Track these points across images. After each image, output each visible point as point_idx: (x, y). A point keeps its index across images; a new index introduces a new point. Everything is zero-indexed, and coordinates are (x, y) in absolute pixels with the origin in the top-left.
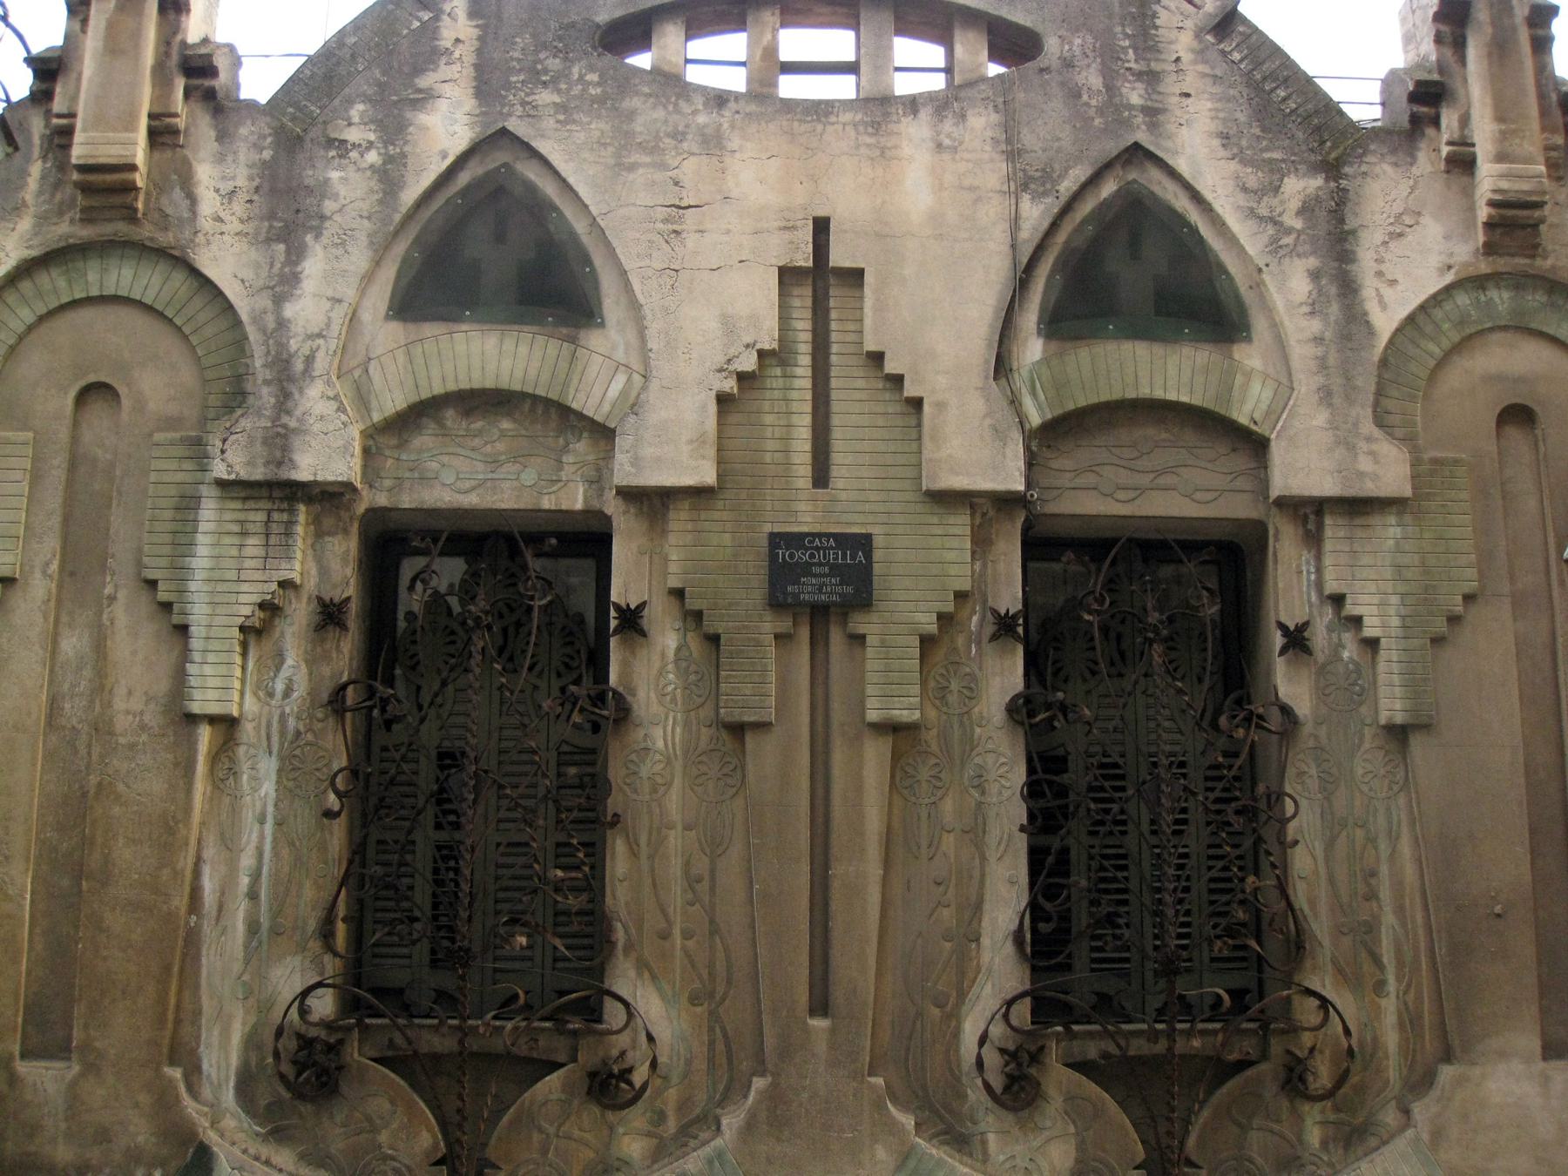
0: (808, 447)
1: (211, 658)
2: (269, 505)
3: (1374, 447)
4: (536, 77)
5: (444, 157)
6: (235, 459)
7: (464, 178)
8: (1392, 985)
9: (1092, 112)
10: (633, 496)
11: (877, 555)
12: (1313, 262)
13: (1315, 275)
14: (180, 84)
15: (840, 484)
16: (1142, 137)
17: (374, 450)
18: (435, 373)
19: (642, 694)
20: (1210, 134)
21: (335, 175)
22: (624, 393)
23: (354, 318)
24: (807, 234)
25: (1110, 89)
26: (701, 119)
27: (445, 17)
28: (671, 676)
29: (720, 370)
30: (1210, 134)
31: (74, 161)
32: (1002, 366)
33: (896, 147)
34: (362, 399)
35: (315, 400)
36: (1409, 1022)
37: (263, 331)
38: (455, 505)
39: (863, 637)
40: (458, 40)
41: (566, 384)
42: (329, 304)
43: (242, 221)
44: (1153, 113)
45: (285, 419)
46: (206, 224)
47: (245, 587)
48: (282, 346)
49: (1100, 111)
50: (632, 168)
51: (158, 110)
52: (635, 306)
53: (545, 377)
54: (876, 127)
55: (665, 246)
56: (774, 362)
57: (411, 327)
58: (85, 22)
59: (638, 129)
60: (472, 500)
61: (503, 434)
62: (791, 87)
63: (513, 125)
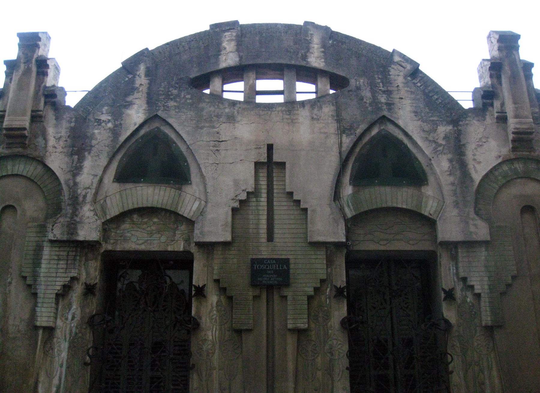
0: (265, 227)
1: (45, 305)
2: (68, 249)
3: (476, 222)
4: (168, 96)
5: (135, 125)
6: (57, 232)
7: (142, 132)
9: (368, 105)
10: (201, 245)
11: (292, 266)
12: (450, 156)
13: (451, 161)
14: (42, 100)
15: (277, 240)
16: (386, 113)
17: (107, 229)
18: (130, 202)
19: (203, 319)
20: (411, 112)
21: (96, 131)
22: (198, 208)
23: (101, 181)
24: (265, 150)
25: (374, 97)
26: (227, 110)
27: (137, 76)
28: (215, 312)
29: (233, 199)
30: (411, 112)
31: (4, 127)
32: (336, 196)
33: (297, 119)
34: (104, 210)
35: (86, 211)
37: (68, 186)
38: (136, 249)
39: (286, 297)
40: (141, 84)
41: (177, 204)
42: (92, 177)
43: (62, 148)
44: (390, 105)
45: (75, 218)
46: (50, 149)
47: (58, 279)
48: (75, 192)
49: (370, 104)
50: (202, 128)
51: (34, 109)
52: (202, 176)
53: (170, 201)
54: (289, 112)
55: (214, 155)
56: (253, 196)
57: (122, 184)
58: (11, 79)
59: (204, 114)
60: (143, 247)
61: (154, 223)
62: (260, 99)
63: (160, 113)
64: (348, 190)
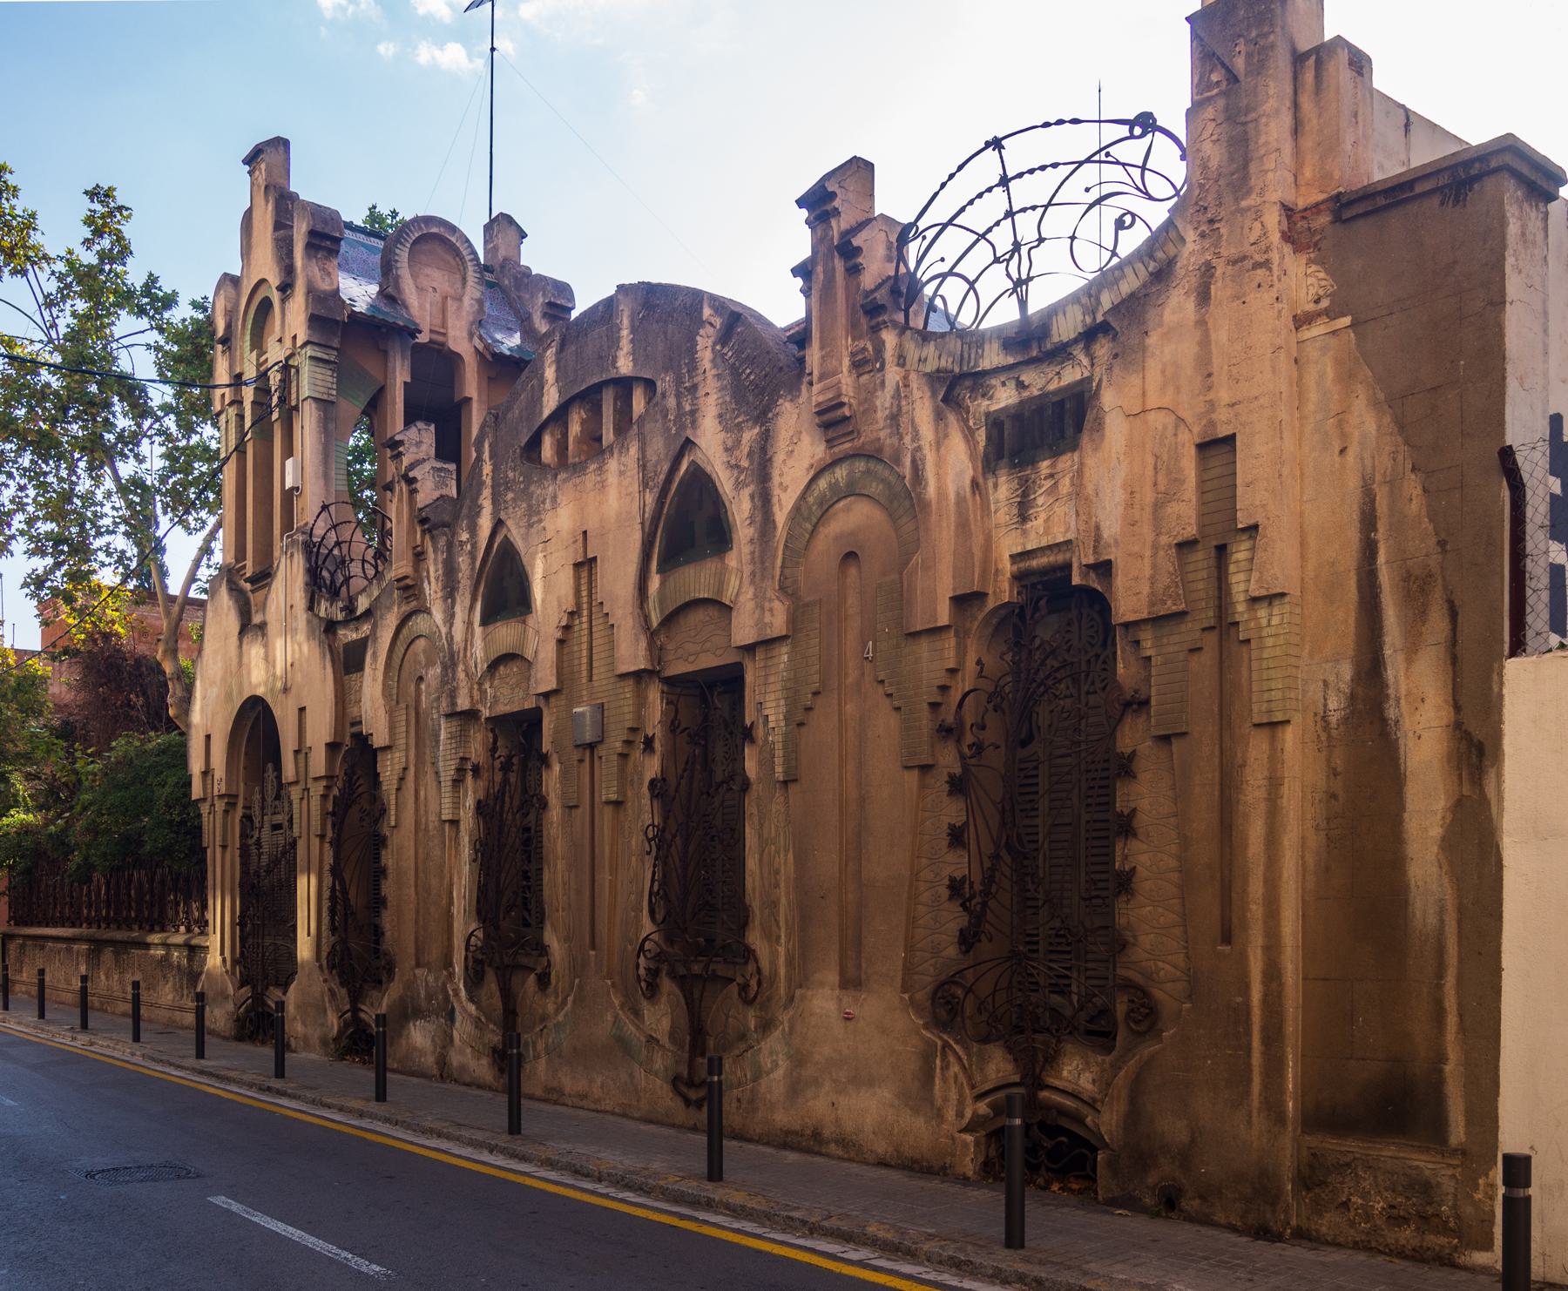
13: (752, 497)
16: (689, 433)
25: (679, 404)
44: (693, 413)
64: (655, 582)
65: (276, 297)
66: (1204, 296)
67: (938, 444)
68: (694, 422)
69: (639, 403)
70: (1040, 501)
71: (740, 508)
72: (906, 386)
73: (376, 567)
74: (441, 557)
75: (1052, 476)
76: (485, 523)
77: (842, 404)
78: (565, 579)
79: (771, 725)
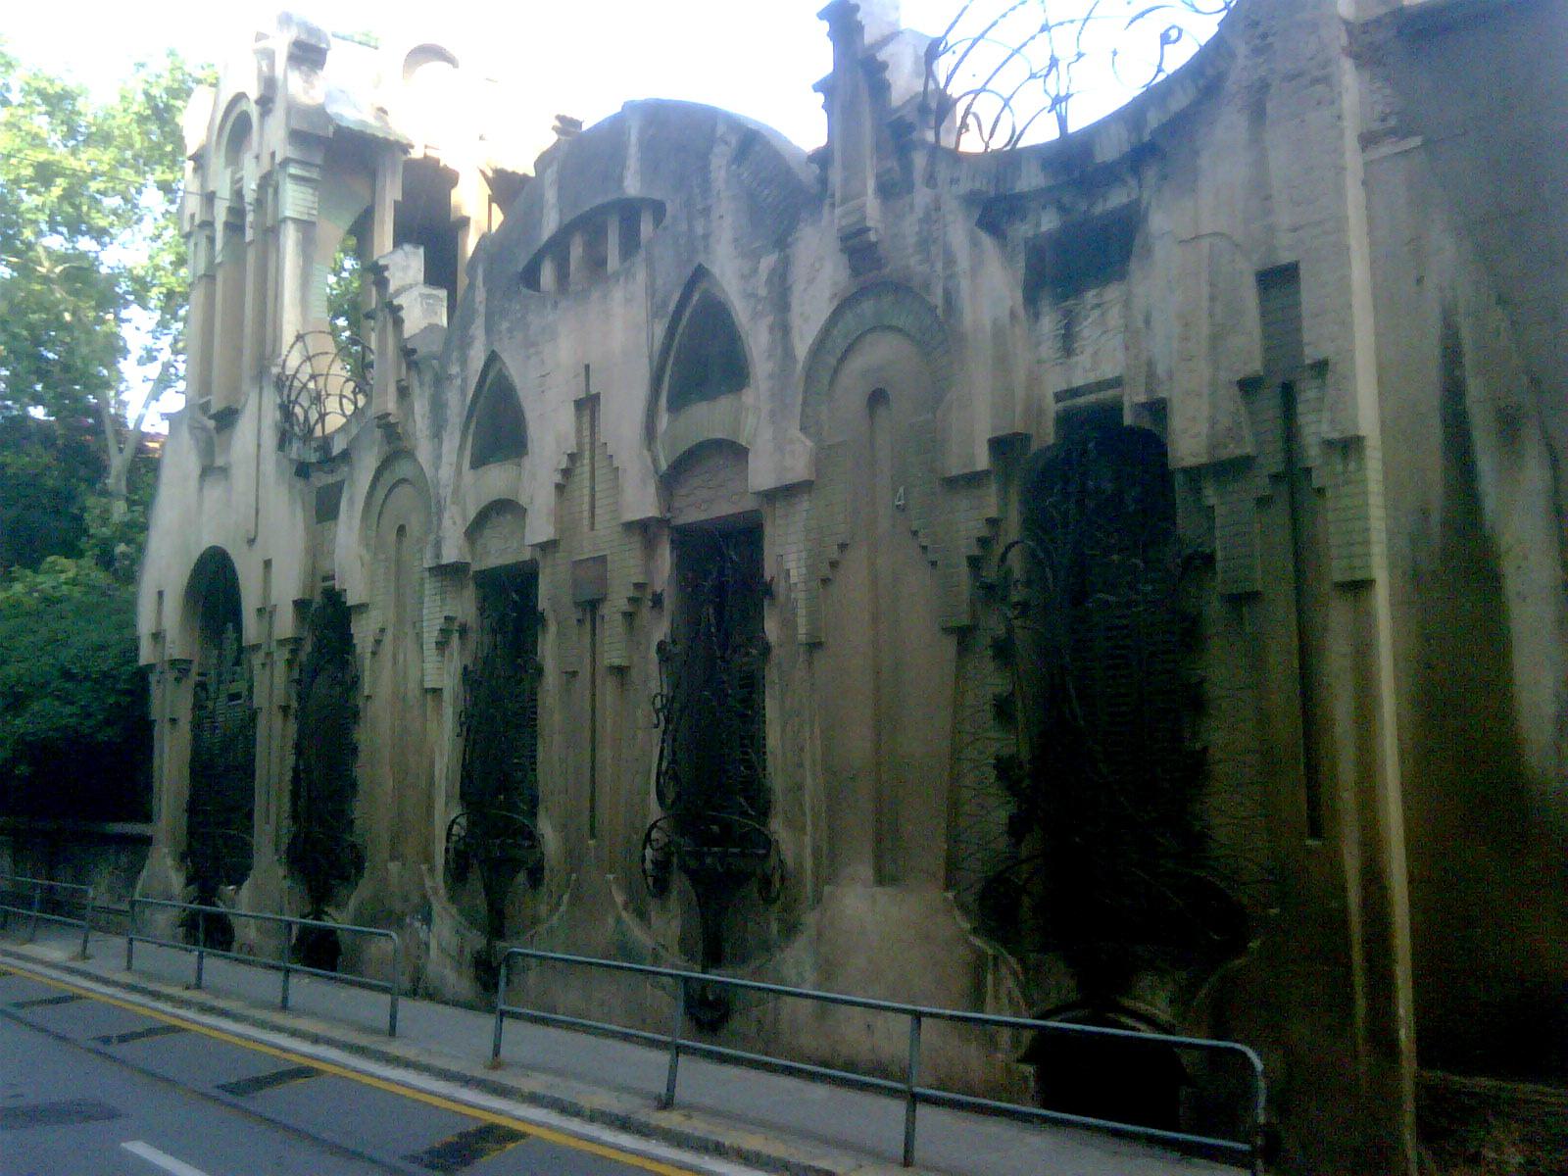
8: (809, 829)
12: (769, 320)
13: (771, 329)
16: (701, 258)
36: (816, 853)
44: (706, 237)
64: (663, 421)
65: (254, 111)
66: (1258, 113)
67: (975, 271)
68: (706, 247)
69: (646, 228)
70: (1086, 333)
71: (758, 341)
72: (938, 209)
73: (355, 403)
74: (428, 393)
75: (1098, 305)
76: (477, 357)
77: (869, 229)
78: (564, 420)
79: (793, 580)
